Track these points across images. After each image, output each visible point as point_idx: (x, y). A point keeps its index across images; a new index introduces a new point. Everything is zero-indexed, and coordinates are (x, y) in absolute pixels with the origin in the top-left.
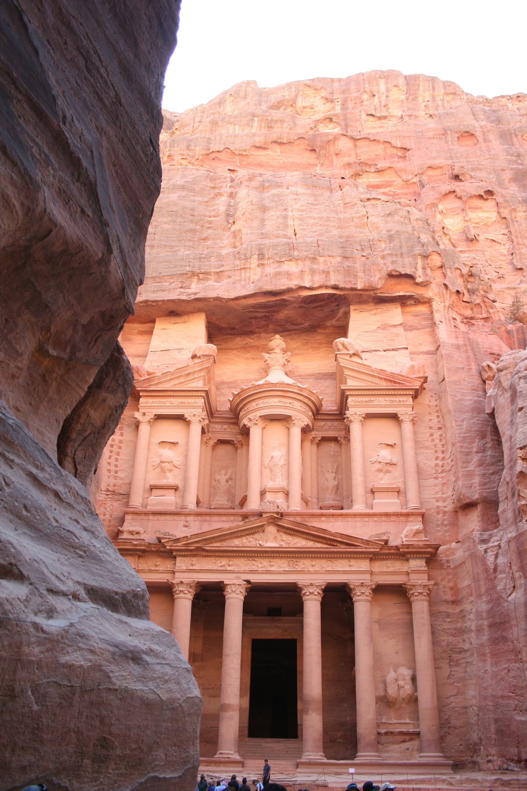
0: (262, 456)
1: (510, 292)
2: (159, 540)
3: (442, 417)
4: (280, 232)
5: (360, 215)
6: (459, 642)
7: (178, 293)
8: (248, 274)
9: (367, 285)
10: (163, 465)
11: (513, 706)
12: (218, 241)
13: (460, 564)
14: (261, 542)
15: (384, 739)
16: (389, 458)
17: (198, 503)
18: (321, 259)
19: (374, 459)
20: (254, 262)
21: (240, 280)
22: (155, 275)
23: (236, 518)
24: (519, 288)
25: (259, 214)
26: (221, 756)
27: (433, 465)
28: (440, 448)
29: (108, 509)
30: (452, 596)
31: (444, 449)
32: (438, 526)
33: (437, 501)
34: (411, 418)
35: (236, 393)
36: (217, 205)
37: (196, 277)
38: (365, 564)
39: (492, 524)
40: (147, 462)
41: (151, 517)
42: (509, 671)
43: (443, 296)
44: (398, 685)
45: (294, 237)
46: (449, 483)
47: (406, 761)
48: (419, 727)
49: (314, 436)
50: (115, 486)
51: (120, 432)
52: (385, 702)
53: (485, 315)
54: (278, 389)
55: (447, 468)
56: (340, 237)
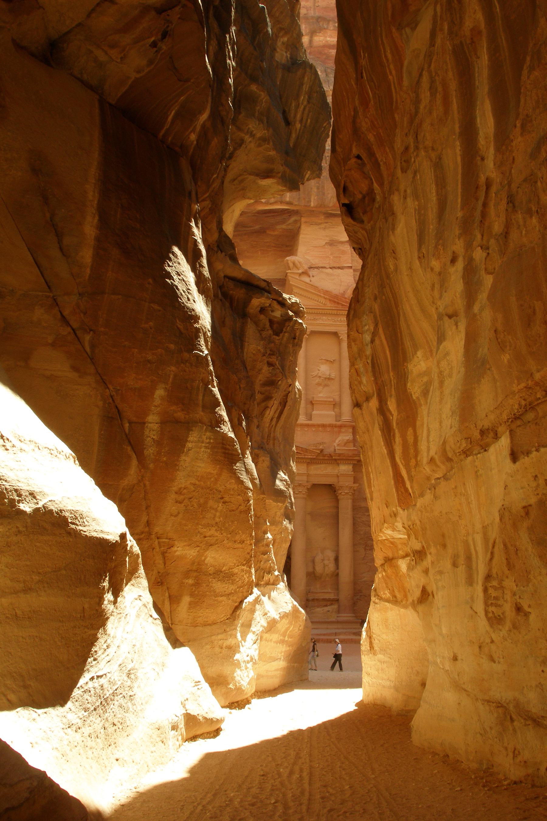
16: (328, 373)
19: (315, 374)
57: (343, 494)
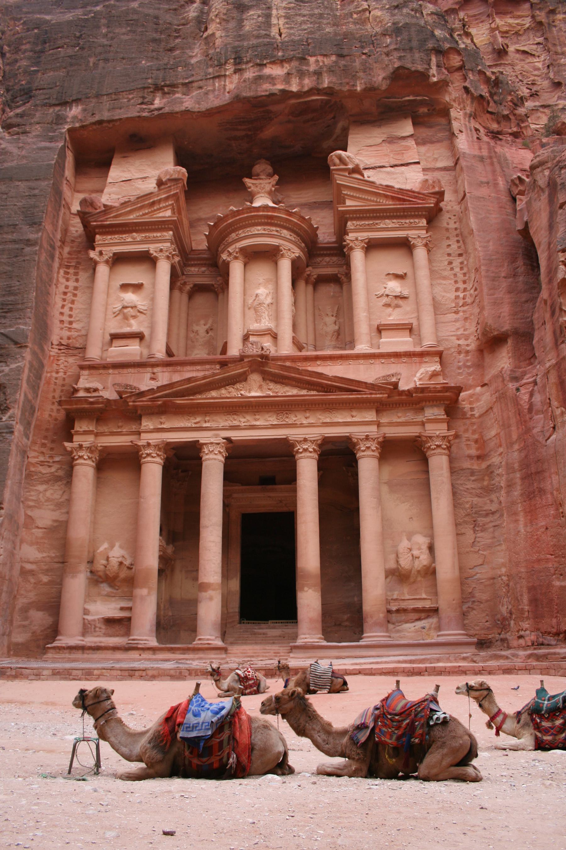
0: (244, 295)
1: (546, 110)
2: (120, 393)
3: (463, 241)
4: (261, 32)
5: (360, 9)
6: (485, 504)
7: (138, 110)
8: (223, 83)
9: (369, 86)
10: (125, 311)
11: (552, 571)
12: (187, 51)
13: (487, 411)
14: (242, 392)
15: (394, 617)
17: (169, 353)
18: (312, 60)
20: (230, 68)
21: (214, 90)
22: (111, 91)
23: (213, 366)
24: (556, 105)
25: (235, 14)
26: (200, 642)
27: (453, 297)
28: (460, 277)
29: (62, 366)
30: (478, 449)
31: (466, 278)
32: (459, 368)
33: (458, 339)
34: (424, 242)
35: (212, 224)
36: (187, 12)
37: (160, 92)
38: (370, 413)
39: (525, 360)
40: (106, 309)
41: (111, 371)
42: (547, 528)
43: (463, 102)
44: (413, 555)
45: (278, 37)
46: (472, 317)
47: (422, 642)
48: (437, 603)
49: (308, 273)
50: (69, 338)
51: (75, 277)
52: (398, 575)
53: (515, 129)
54: (261, 213)
55: (469, 300)
56: (336, 34)
57: (433, 447)
